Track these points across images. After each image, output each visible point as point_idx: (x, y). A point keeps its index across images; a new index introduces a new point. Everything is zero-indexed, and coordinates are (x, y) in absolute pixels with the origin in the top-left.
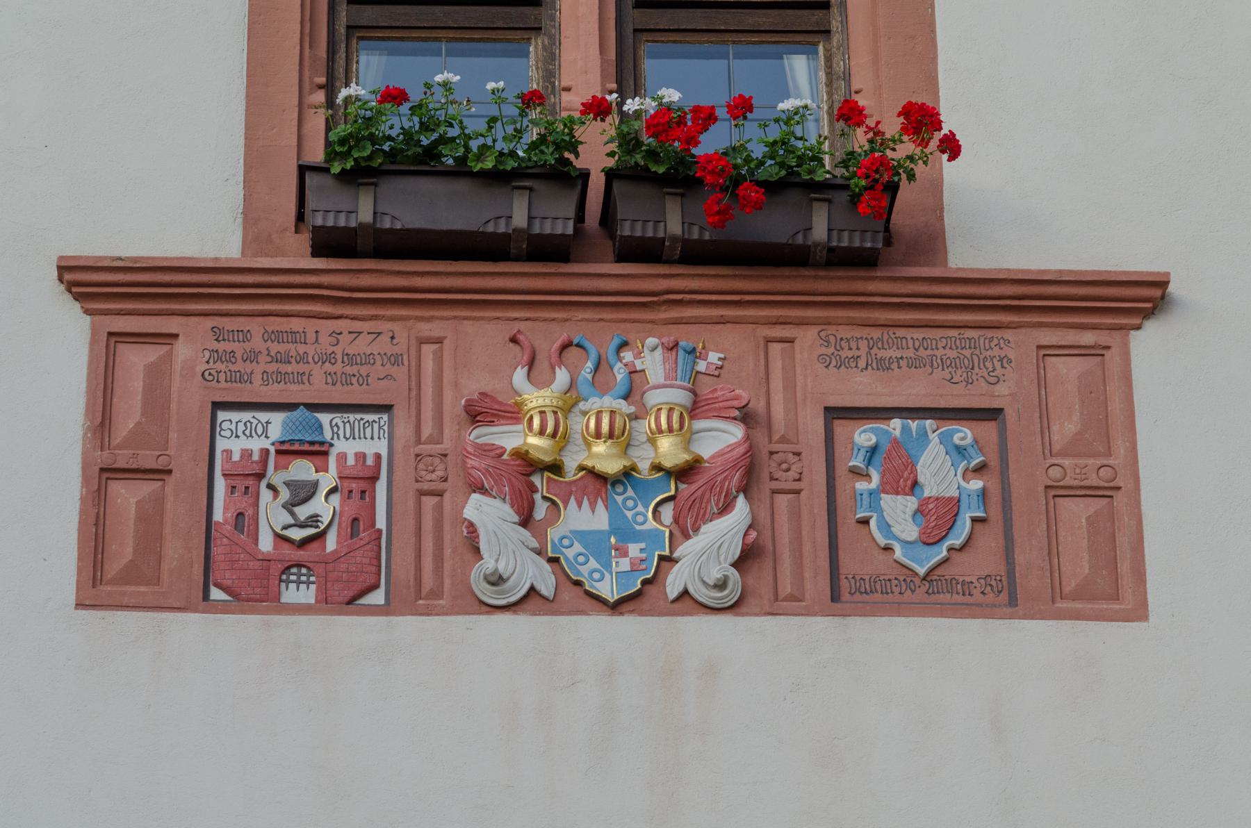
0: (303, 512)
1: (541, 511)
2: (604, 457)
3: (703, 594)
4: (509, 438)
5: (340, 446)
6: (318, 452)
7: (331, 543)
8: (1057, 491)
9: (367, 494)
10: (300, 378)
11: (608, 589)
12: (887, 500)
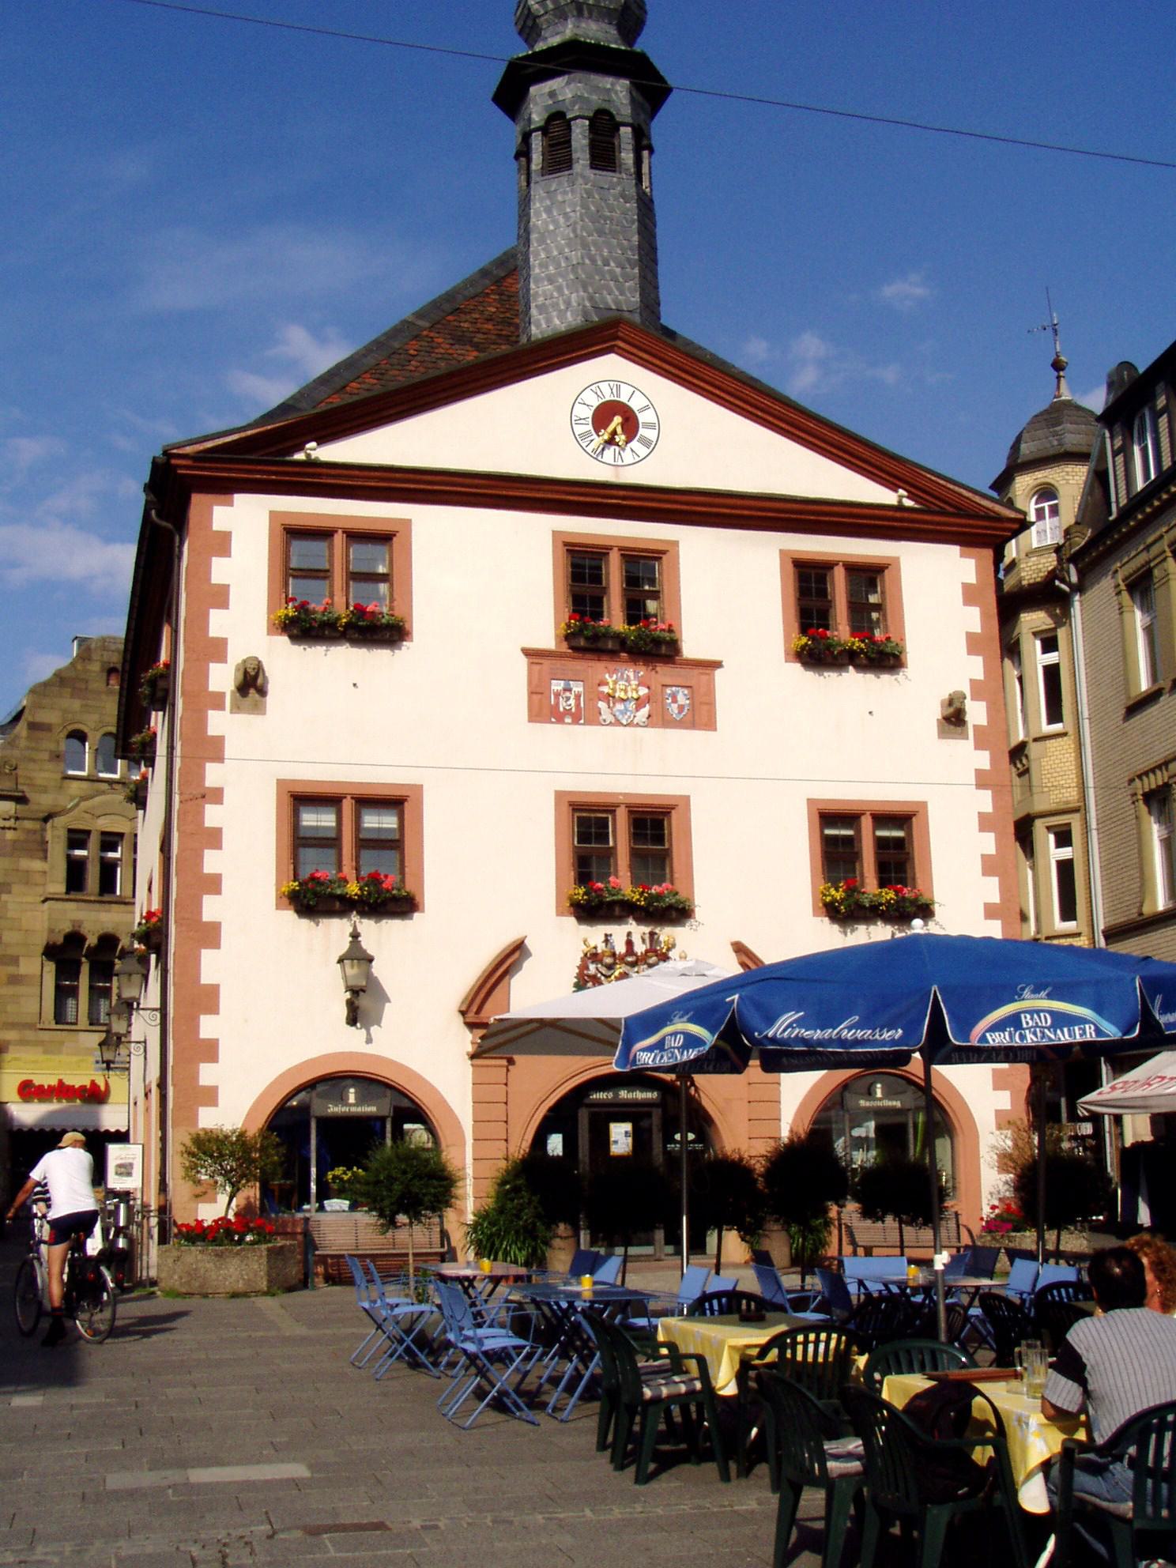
0: (569, 703)
1: (611, 705)
2: (622, 695)
3: (642, 724)
4: (605, 689)
5: (574, 689)
6: (570, 690)
7: (573, 710)
8: (701, 703)
9: (579, 700)
11: (625, 722)
12: (672, 705)
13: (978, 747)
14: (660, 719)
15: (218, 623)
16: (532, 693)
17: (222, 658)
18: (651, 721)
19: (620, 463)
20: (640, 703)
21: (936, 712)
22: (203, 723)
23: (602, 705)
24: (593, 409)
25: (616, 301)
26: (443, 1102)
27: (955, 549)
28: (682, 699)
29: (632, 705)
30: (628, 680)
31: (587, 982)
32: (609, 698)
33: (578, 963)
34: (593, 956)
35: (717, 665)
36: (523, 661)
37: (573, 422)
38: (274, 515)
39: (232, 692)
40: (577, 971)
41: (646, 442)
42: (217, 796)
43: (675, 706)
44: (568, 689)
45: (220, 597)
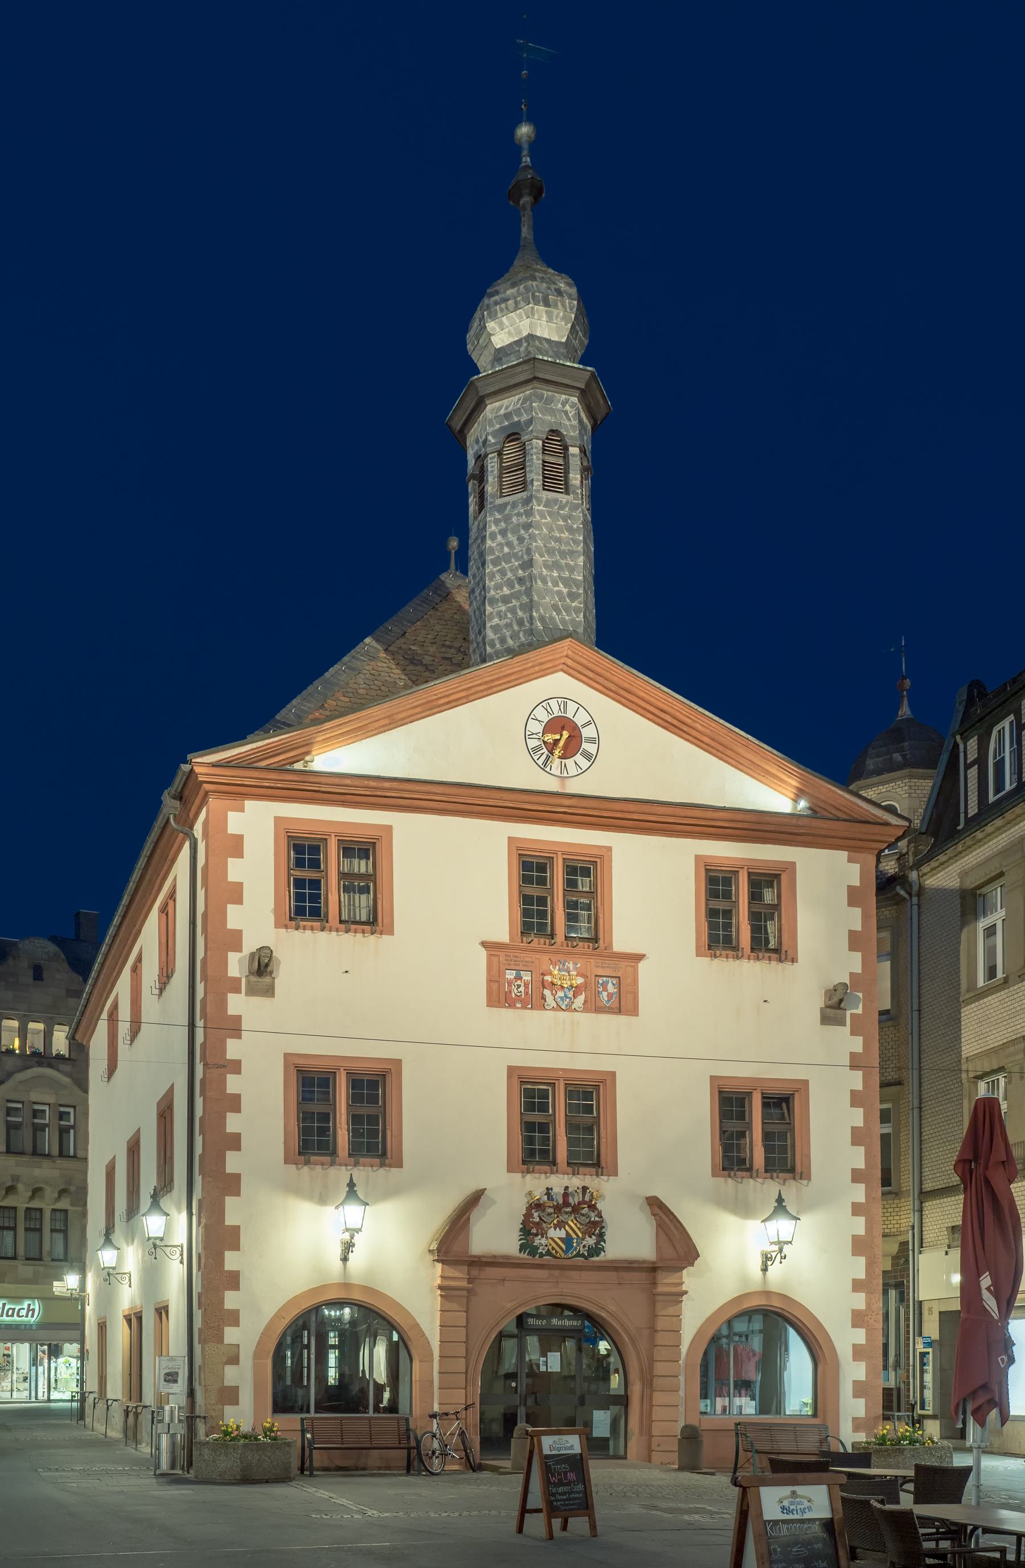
0: (519, 990)
5: (524, 978)
10: (518, 965)
11: (564, 1007)
14: (594, 1007)
15: (235, 917)
16: (490, 981)
17: (239, 949)
18: (587, 1008)
19: (565, 775)
20: (577, 990)
22: (223, 1004)
24: (543, 724)
25: (563, 621)
26: (416, 1326)
28: (611, 988)
34: (538, 1206)
35: (640, 957)
36: (483, 953)
37: (527, 737)
38: (278, 820)
40: (523, 1218)
41: (588, 756)
42: (236, 1067)
43: (605, 994)
44: (518, 977)
45: (236, 894)
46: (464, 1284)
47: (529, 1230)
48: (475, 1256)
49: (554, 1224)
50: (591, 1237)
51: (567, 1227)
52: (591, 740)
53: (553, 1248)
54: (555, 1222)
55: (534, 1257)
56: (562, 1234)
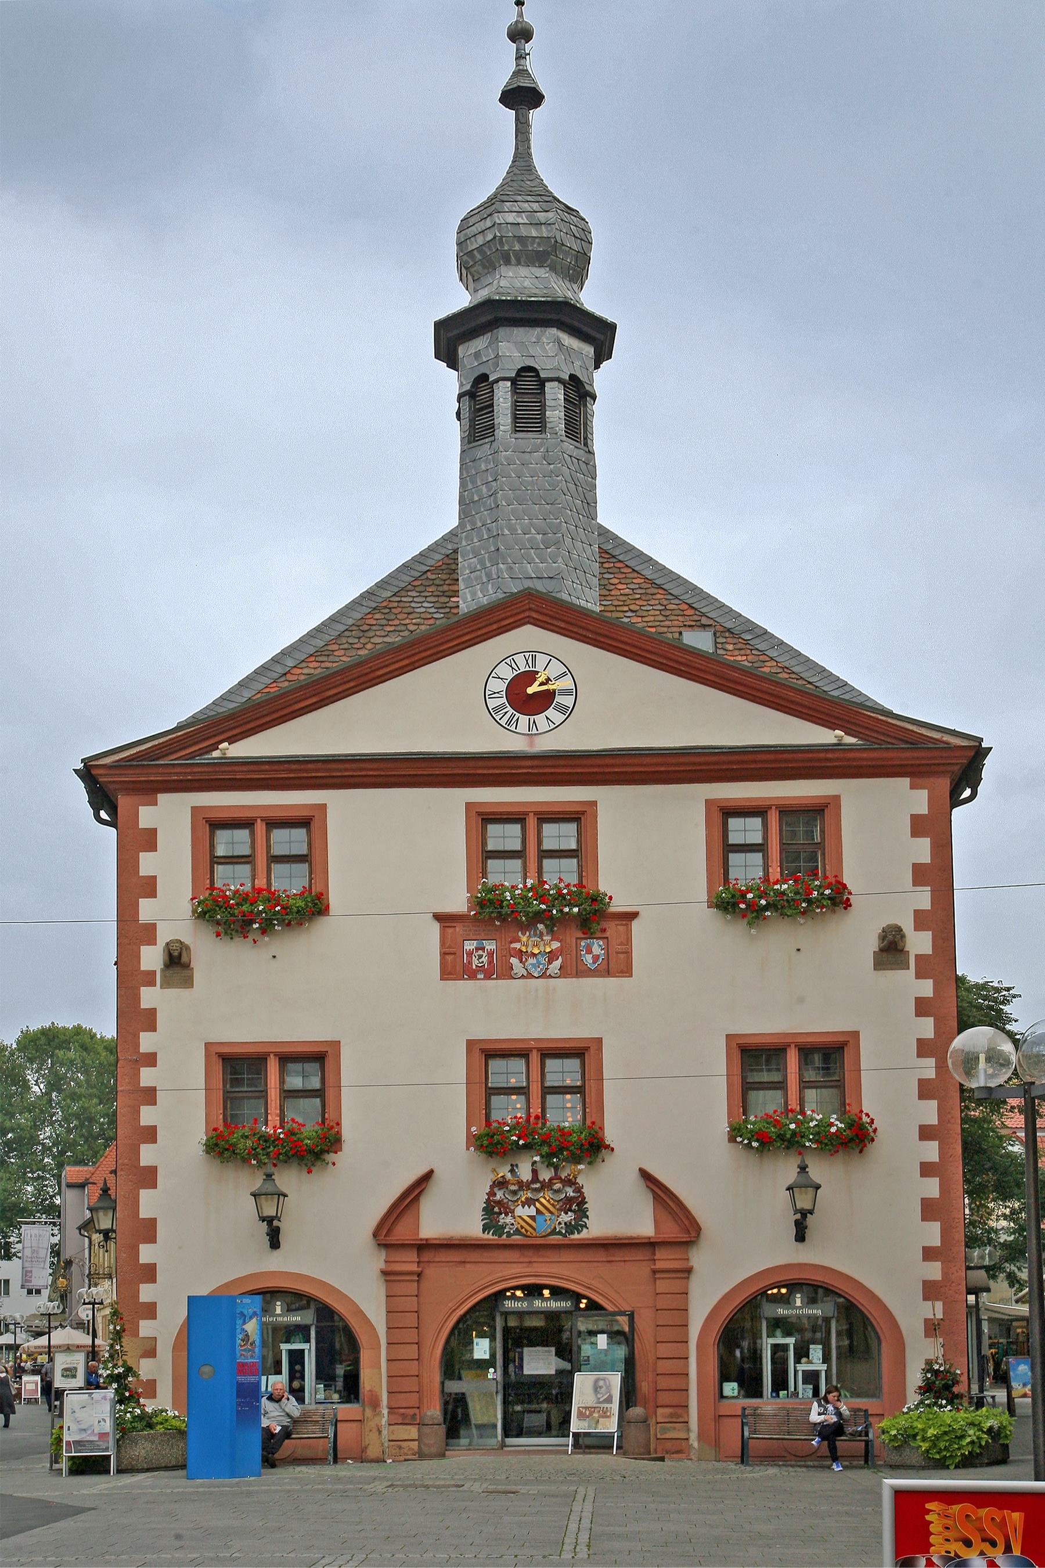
0: (481, 961)
1: (524, 960)
2: (536, 951)
4: (517, 945)
6: (483, 949)
7: (486, 967)
13: (919, 976)
14: (574, 970)
16: (443, 954)
17: (152, 941)
18: (564, 972)
19: (535, 731)
20: (552, 956)
21: (873, 944)
23: (514, 961)
27: (904, 783)
28: (596, 950)
29: (543, 960)
30: (541, 935)
31: (495, 1207)
32: (520, 954)
33: (488, 1190)
35: (634, 915)
36: (436, 926)
37: (487, 697)
38: (195, 810)
39: (162, 970)
46: (414, 1268)
47: (492, 1210)
48: (421, 1240)
49: (521, 1202)
50: (566, 1213)
51: (537, 1204)
52: (566, 692)
53: (522, 1227)
54: (523, 1199)
55: (500, 1236)
56: (532, 1211)
